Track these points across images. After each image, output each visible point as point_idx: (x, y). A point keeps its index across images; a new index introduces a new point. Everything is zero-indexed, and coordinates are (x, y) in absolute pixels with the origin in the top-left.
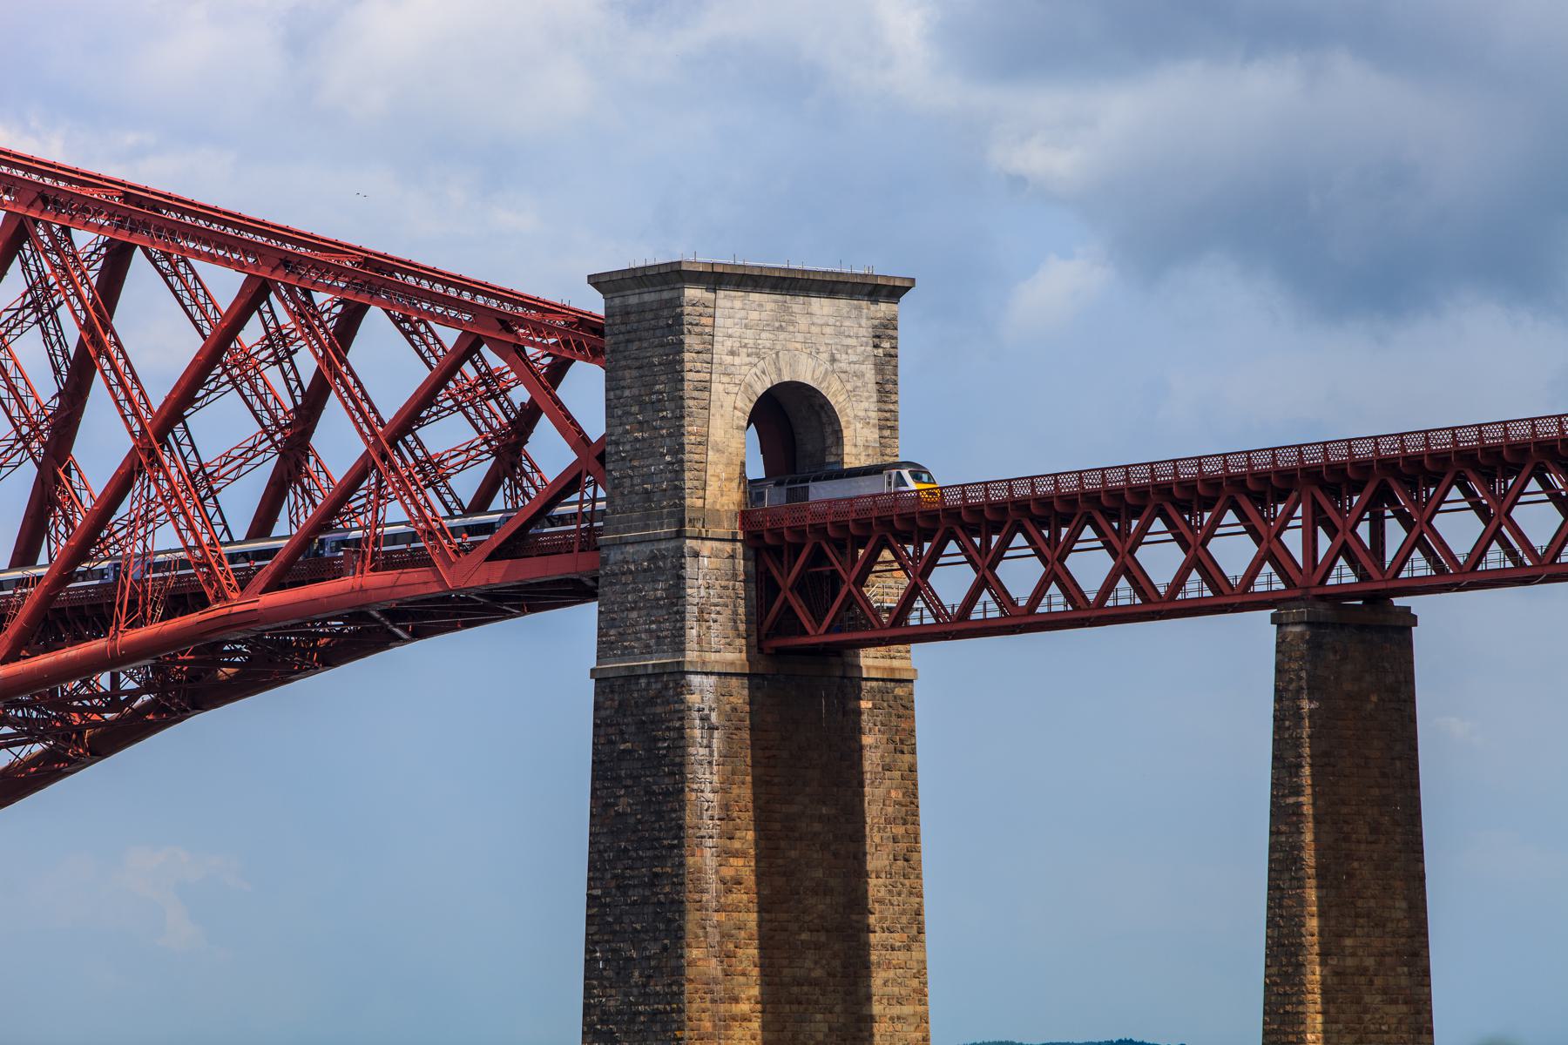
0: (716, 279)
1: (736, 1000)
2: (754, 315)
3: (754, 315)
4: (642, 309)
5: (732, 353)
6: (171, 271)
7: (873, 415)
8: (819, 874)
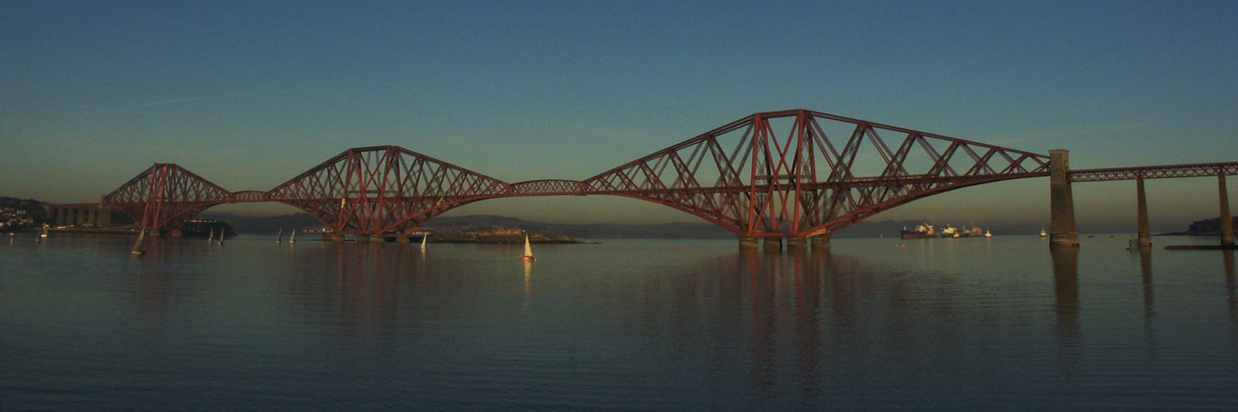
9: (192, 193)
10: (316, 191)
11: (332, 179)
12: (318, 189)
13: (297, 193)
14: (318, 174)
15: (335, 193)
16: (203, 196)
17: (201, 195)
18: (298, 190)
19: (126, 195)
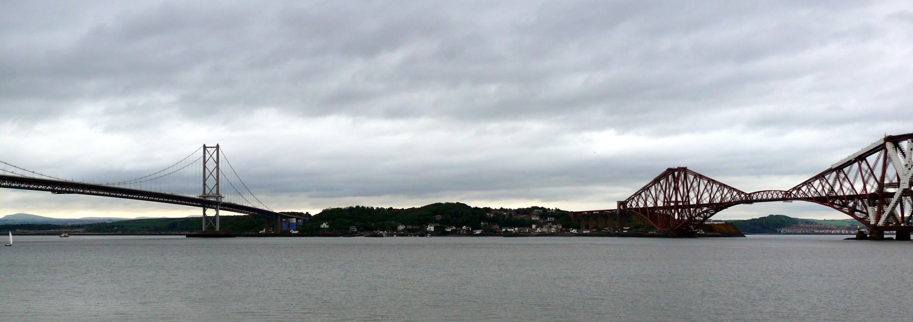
9: (706, 195)
10: (846, 187)
11: (864, 173)
12: (846, 185)
13: (823, 189)
14: (846, 170)
15: (868, 187)
16: (717, 198)
17: (715, 197)
18: (823, 187)
19: (641, 200)
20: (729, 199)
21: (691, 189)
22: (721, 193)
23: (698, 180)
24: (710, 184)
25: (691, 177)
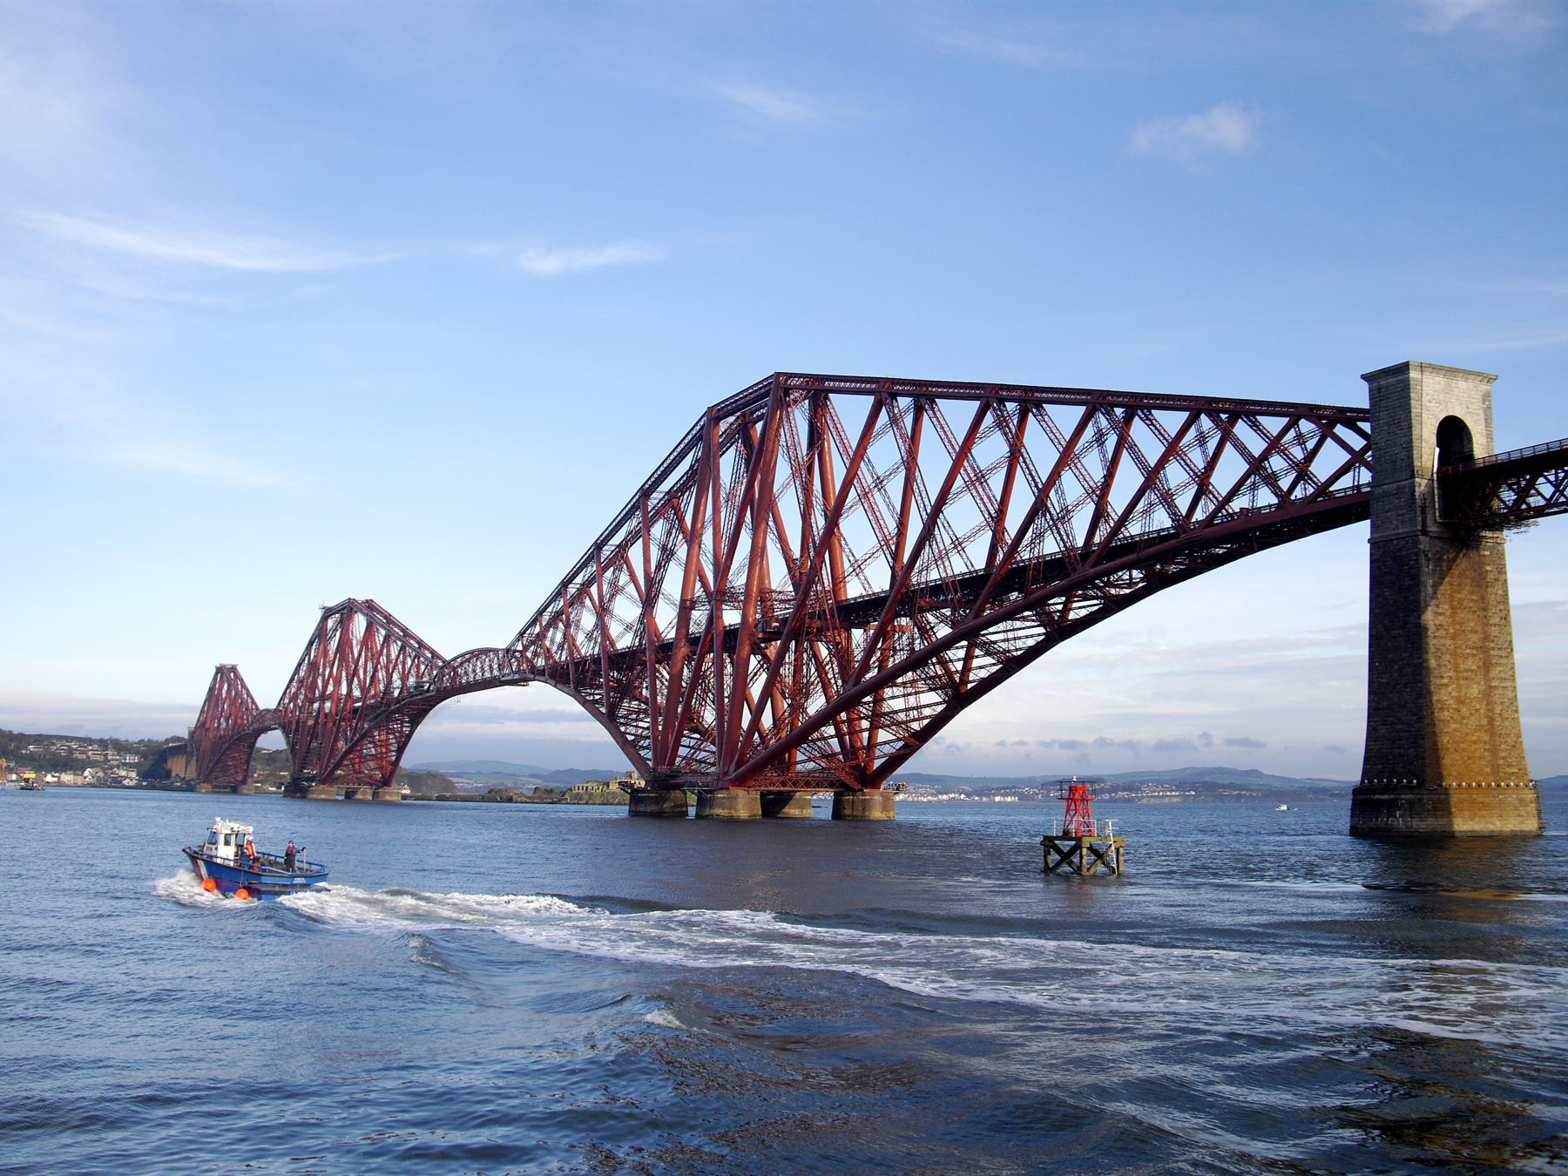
0: (1422, 367)
1: (1442, 677)
2: (1437, 386)
3: (1437, 386)
4: (1388, 386)
5: (1430, 402)
6: (1150, 422)
7: (1484, 433)
8: (1472, 624)
16: (1066, 514)
20: (1183, 503)
21: (852, 494)
22: (1098, 474)
23: (908, 421)
24: (1001, 424)
25: (850, 411)
